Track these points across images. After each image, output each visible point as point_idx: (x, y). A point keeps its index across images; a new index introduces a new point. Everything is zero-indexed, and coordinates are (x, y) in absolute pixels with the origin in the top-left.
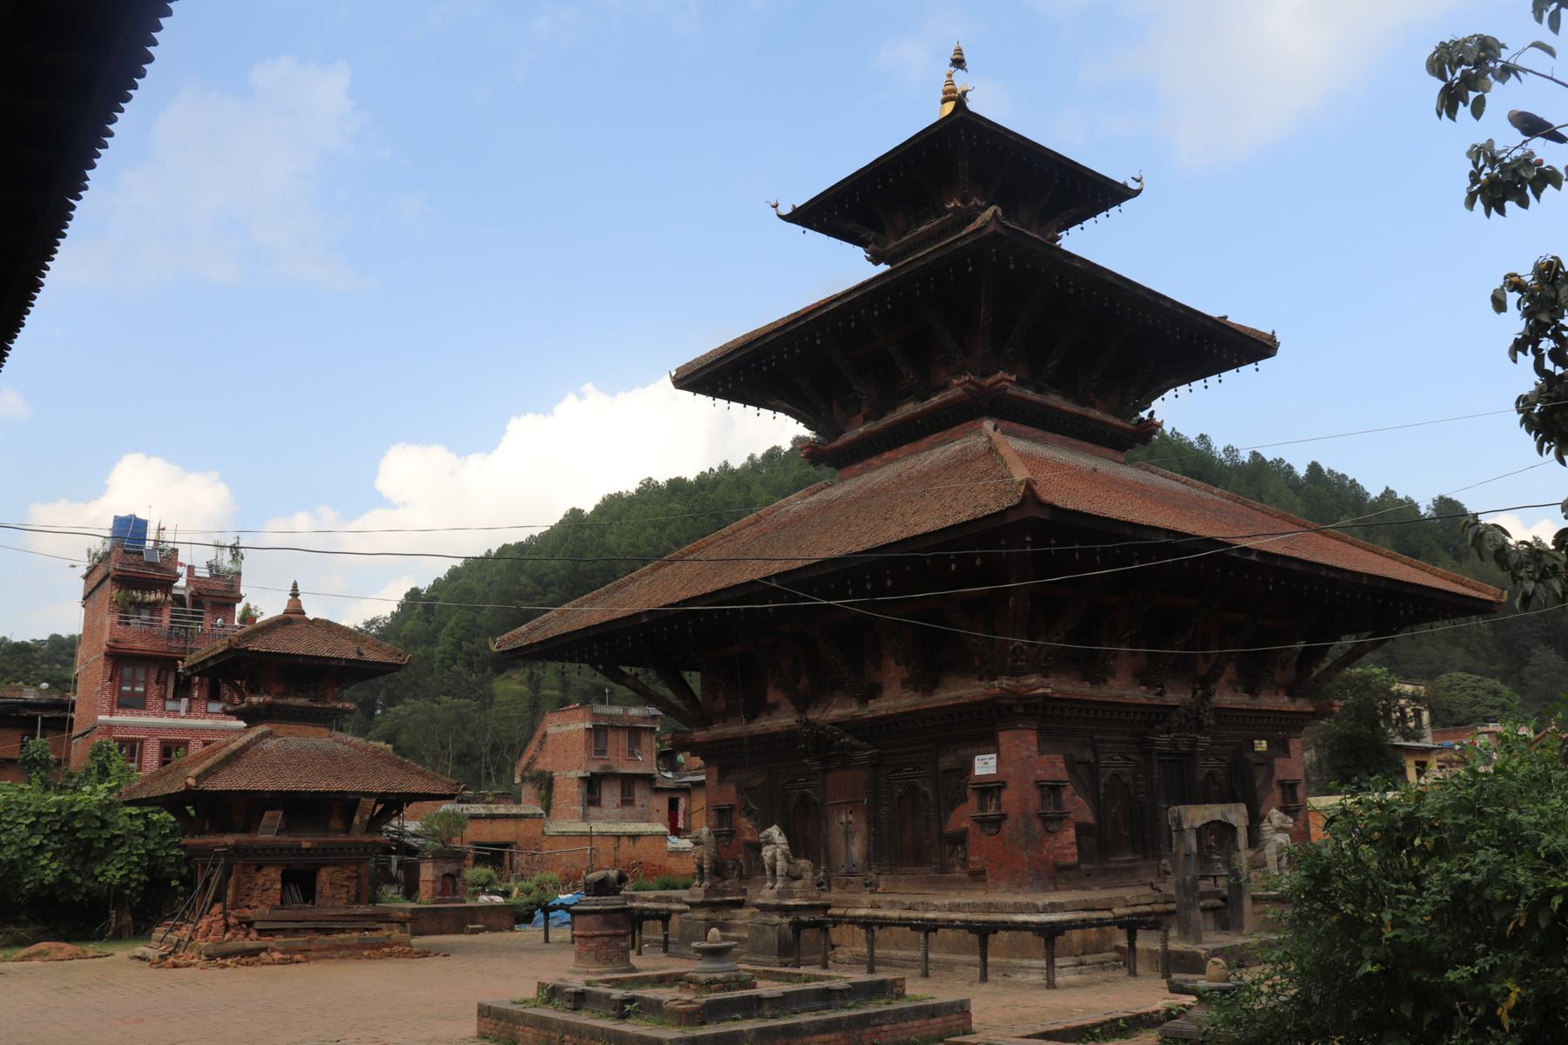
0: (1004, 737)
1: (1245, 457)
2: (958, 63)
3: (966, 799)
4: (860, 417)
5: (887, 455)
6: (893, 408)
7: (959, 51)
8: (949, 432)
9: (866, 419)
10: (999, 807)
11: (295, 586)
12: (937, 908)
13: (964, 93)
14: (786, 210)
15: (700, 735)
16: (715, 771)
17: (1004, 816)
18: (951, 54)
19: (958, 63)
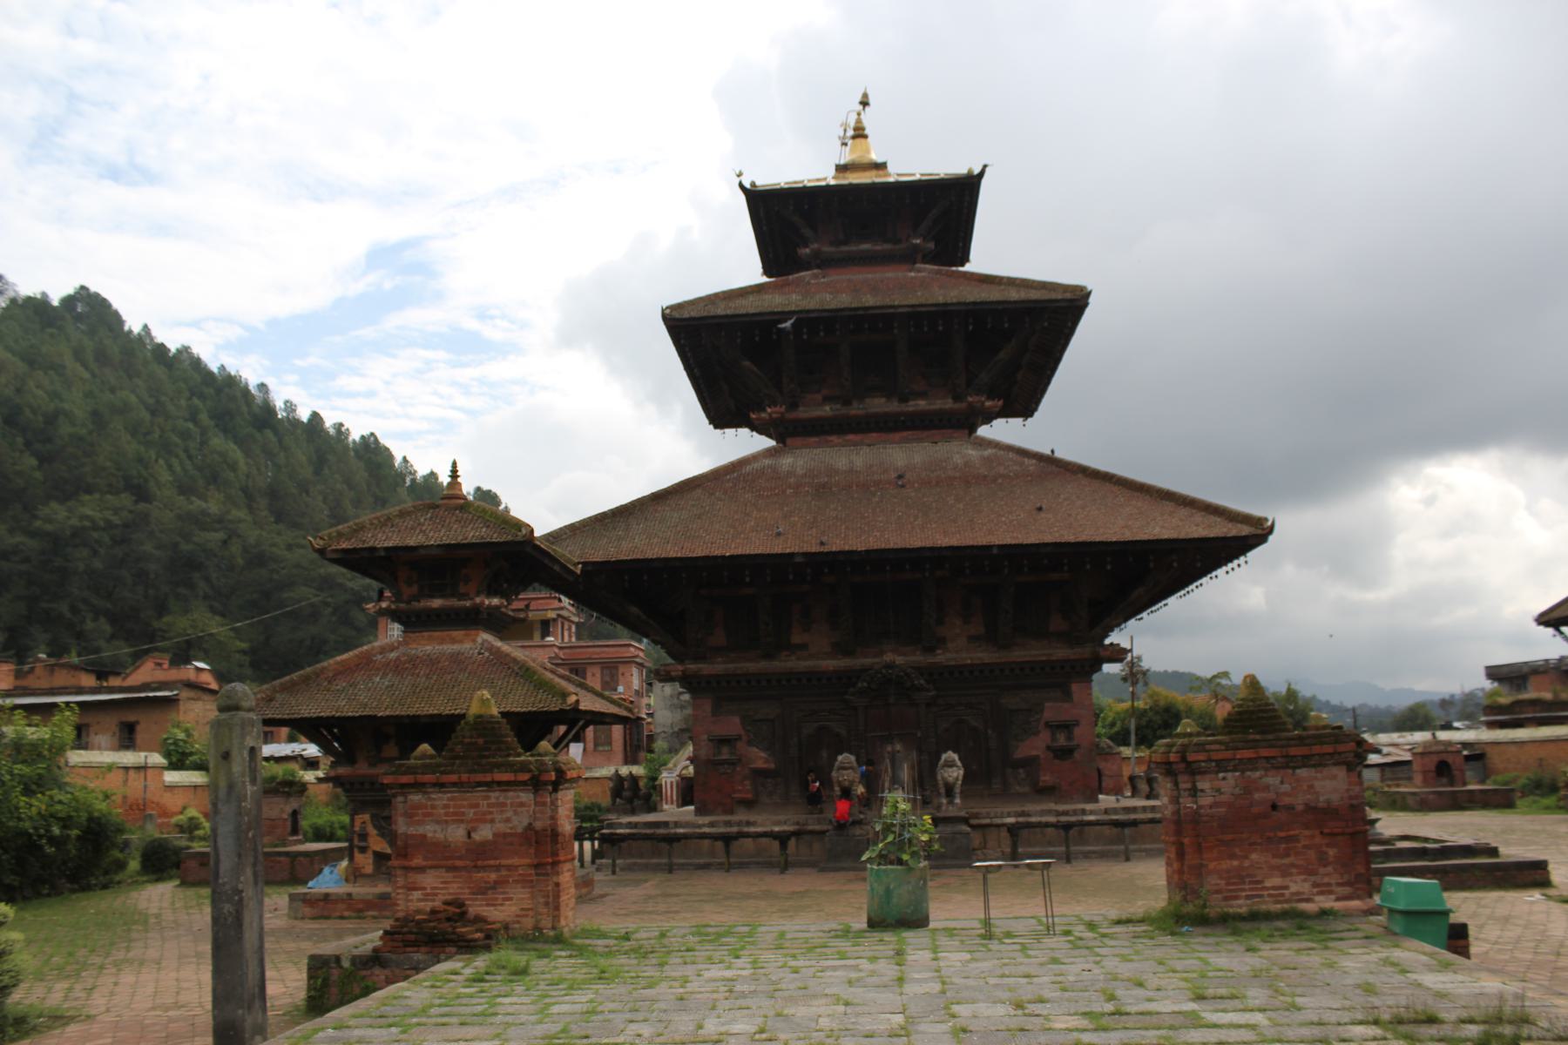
0: (1075, 687)
1: (304, 415)
2: (865, 103)
3: (1037, 733)
4: (819, 397)
5: (850, 437)
7: (865, 95)
8: (926, 433)
10: (1069, 738)
11: (454, 464)
12: (1091, 812)
13: (985, 166)
15: (706, 668)
16: (707, 706)
18: (859, 98)
19: (865, 103)
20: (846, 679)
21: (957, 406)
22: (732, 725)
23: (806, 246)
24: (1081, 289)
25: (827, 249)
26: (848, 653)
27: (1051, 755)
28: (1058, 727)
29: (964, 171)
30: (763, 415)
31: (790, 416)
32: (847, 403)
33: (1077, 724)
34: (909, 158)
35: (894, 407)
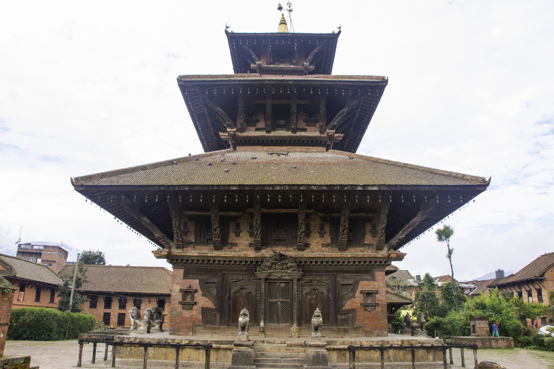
6: (274, 130)
9: (258, 130)
14: (229, 30)
16: (182, 271)
17: (378, 304)
20: (256, 263)
21: (322, 135)
22: (195, 283)
23: (255, 64)
24: (383, 78)
25: (265, 65)
26: (258, 249)
27: (363, 308)
28: (367, 294)
29: (331, 32)
30: (226, 134)
31: (239, 134)
32: (268, 132)
33: (377, 293)
34: (303, 24)
35: (289, 134)
